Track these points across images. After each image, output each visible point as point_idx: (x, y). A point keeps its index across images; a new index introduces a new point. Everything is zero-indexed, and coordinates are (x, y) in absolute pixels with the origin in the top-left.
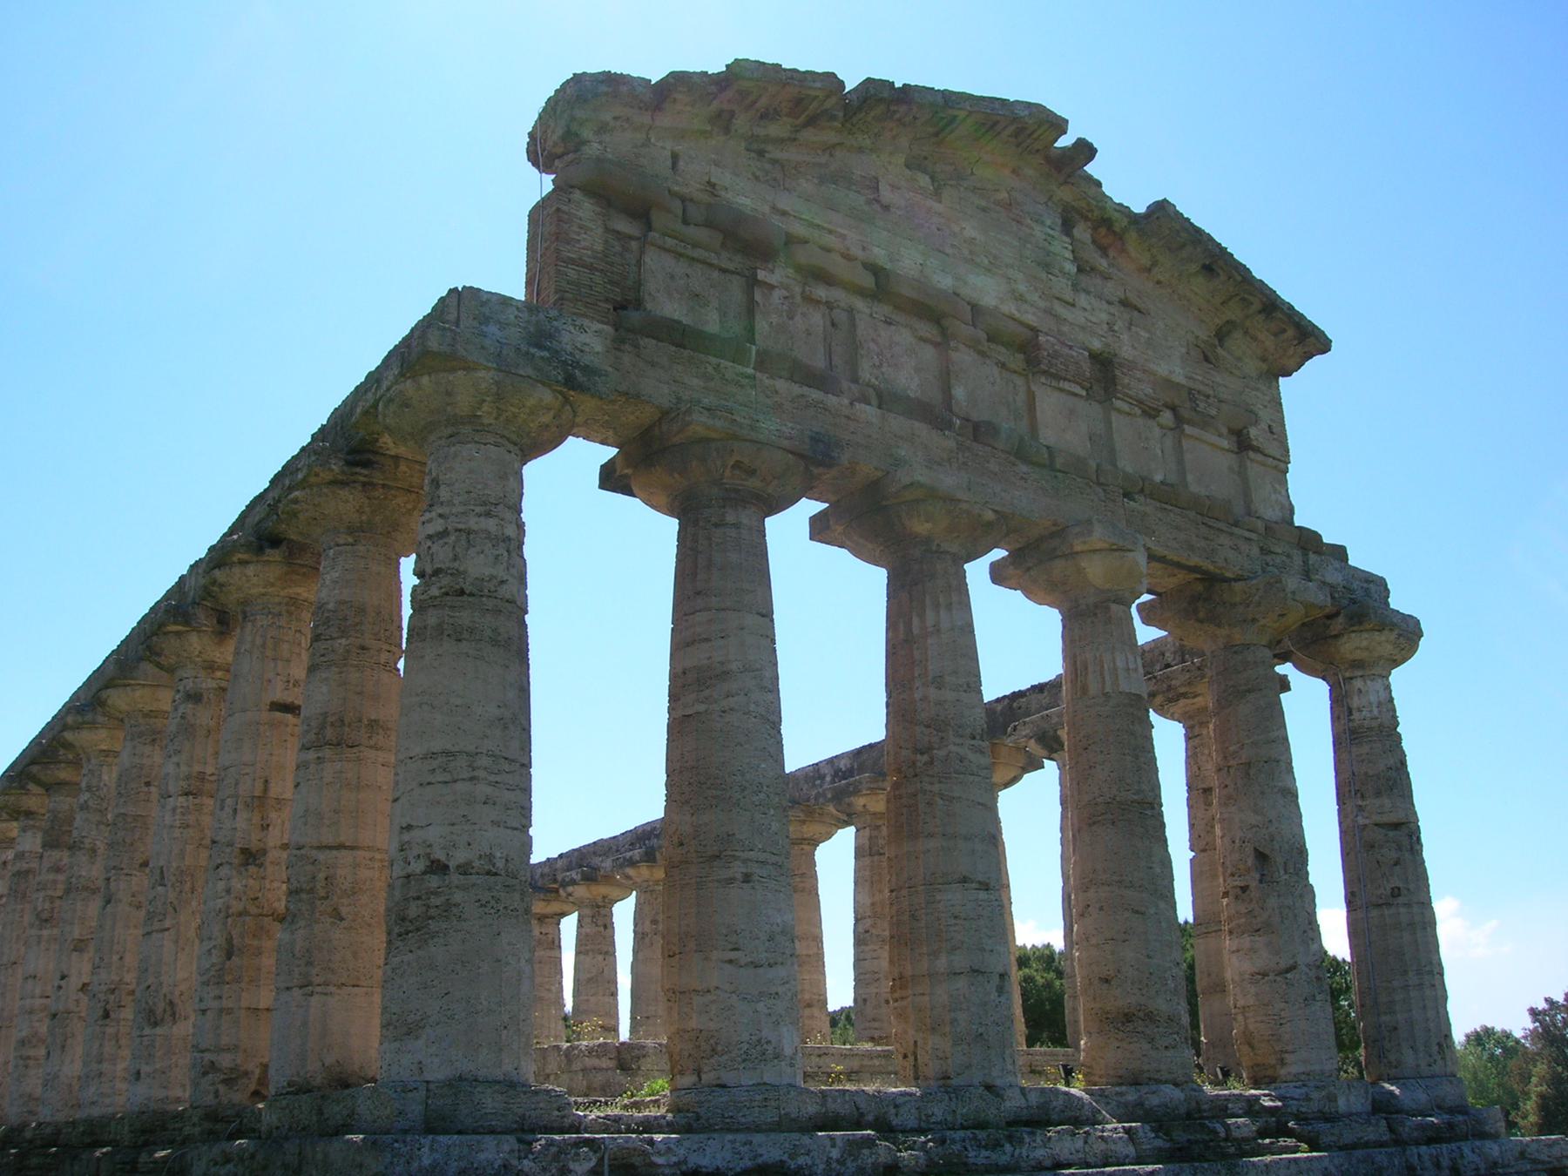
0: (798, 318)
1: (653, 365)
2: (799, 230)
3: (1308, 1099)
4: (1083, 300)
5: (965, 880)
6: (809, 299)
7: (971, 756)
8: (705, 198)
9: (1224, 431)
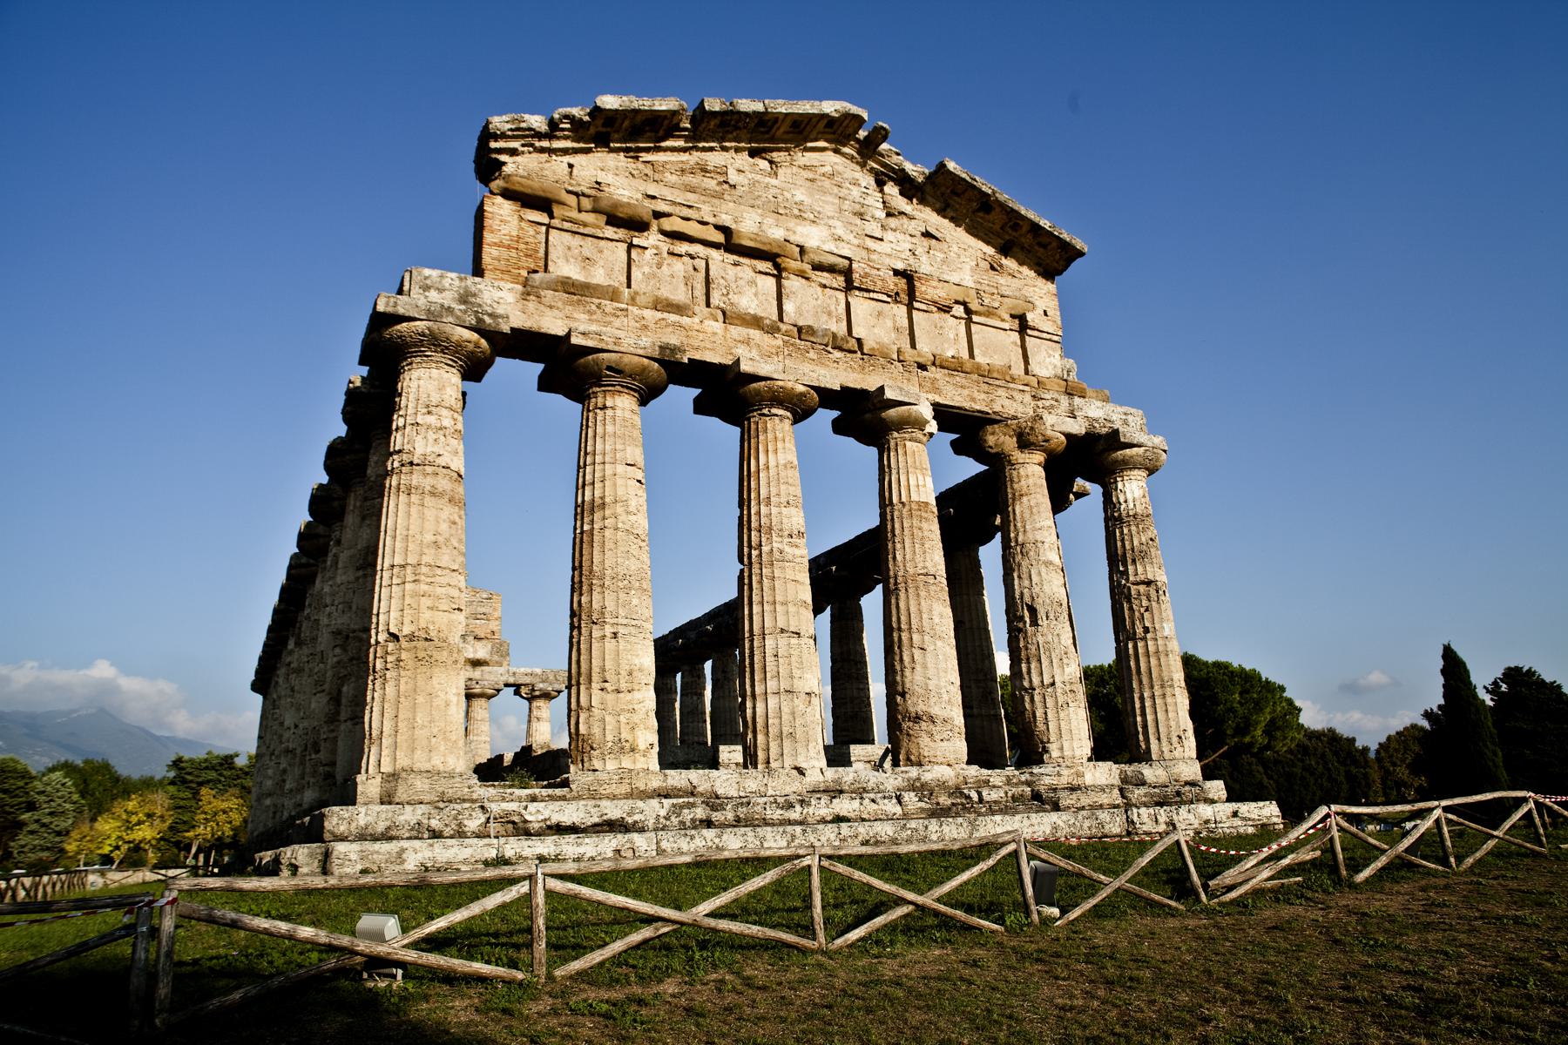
0: (664, 268)
1: (551, 307)
2: (662, 207)
3: (1059, 775)
4: (889, 236)
5: (782, 631)
6: (671, 254)
7: (787, 549)
8: (593, 192)
9: (1007, 317)
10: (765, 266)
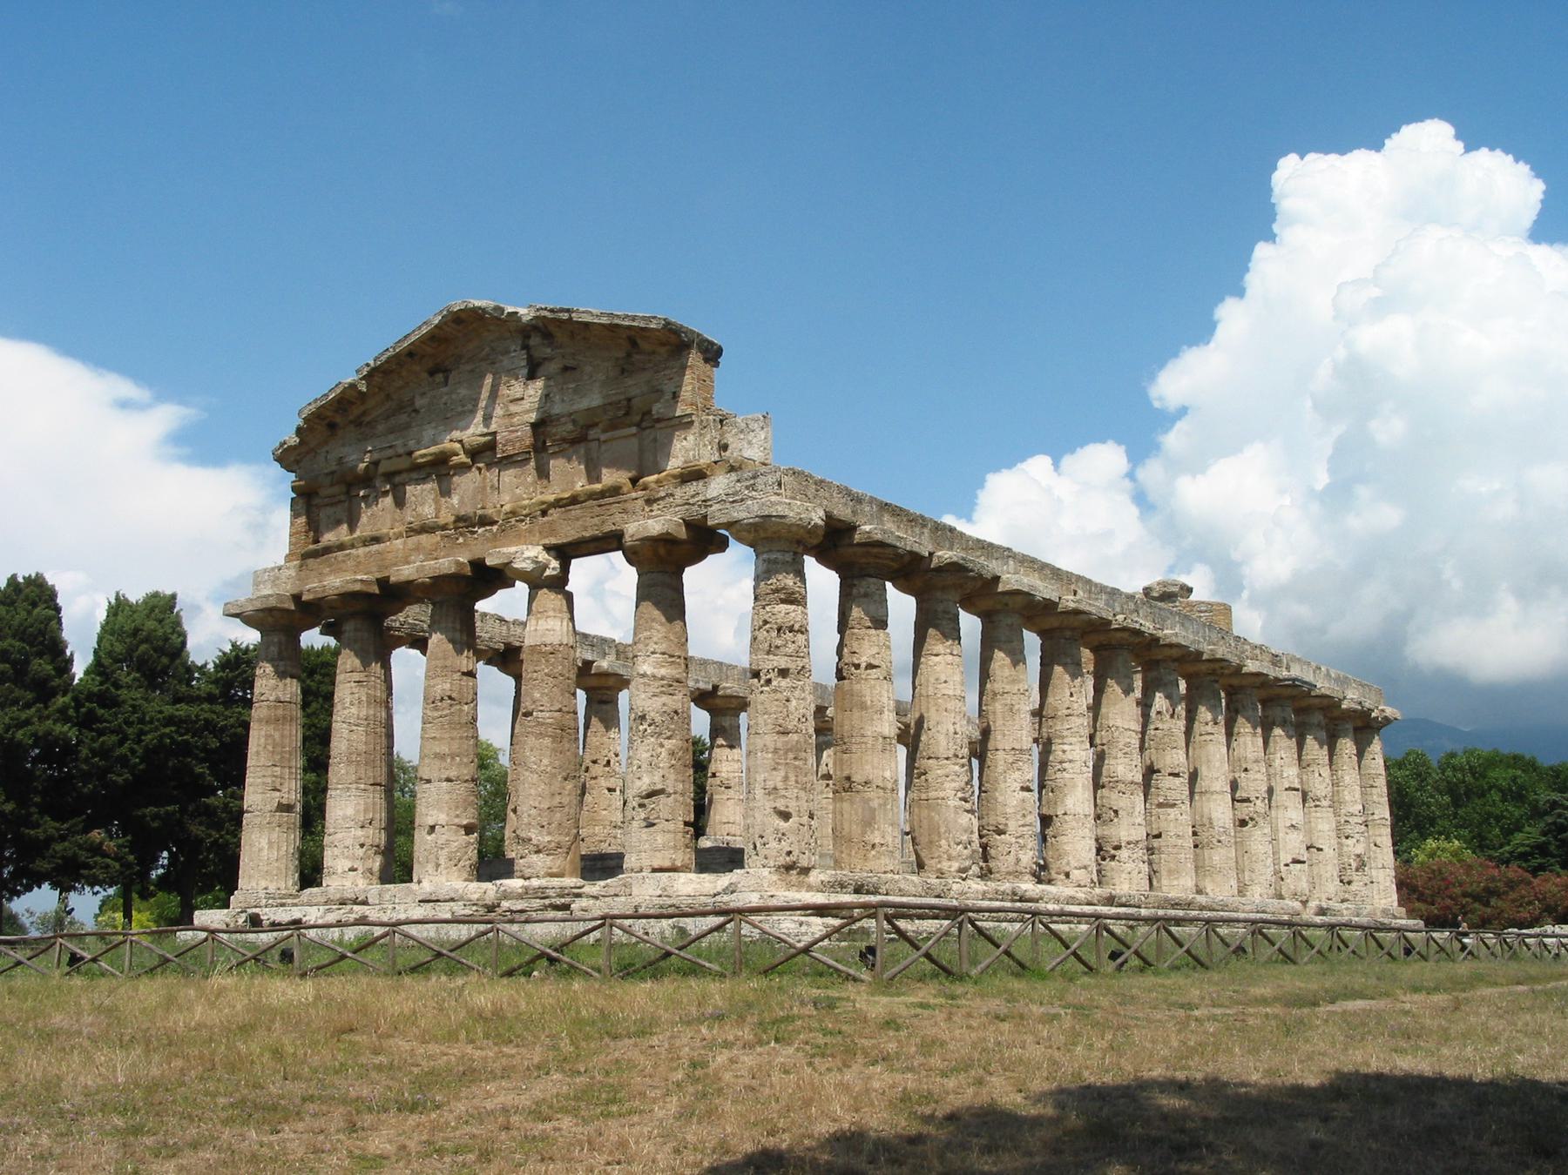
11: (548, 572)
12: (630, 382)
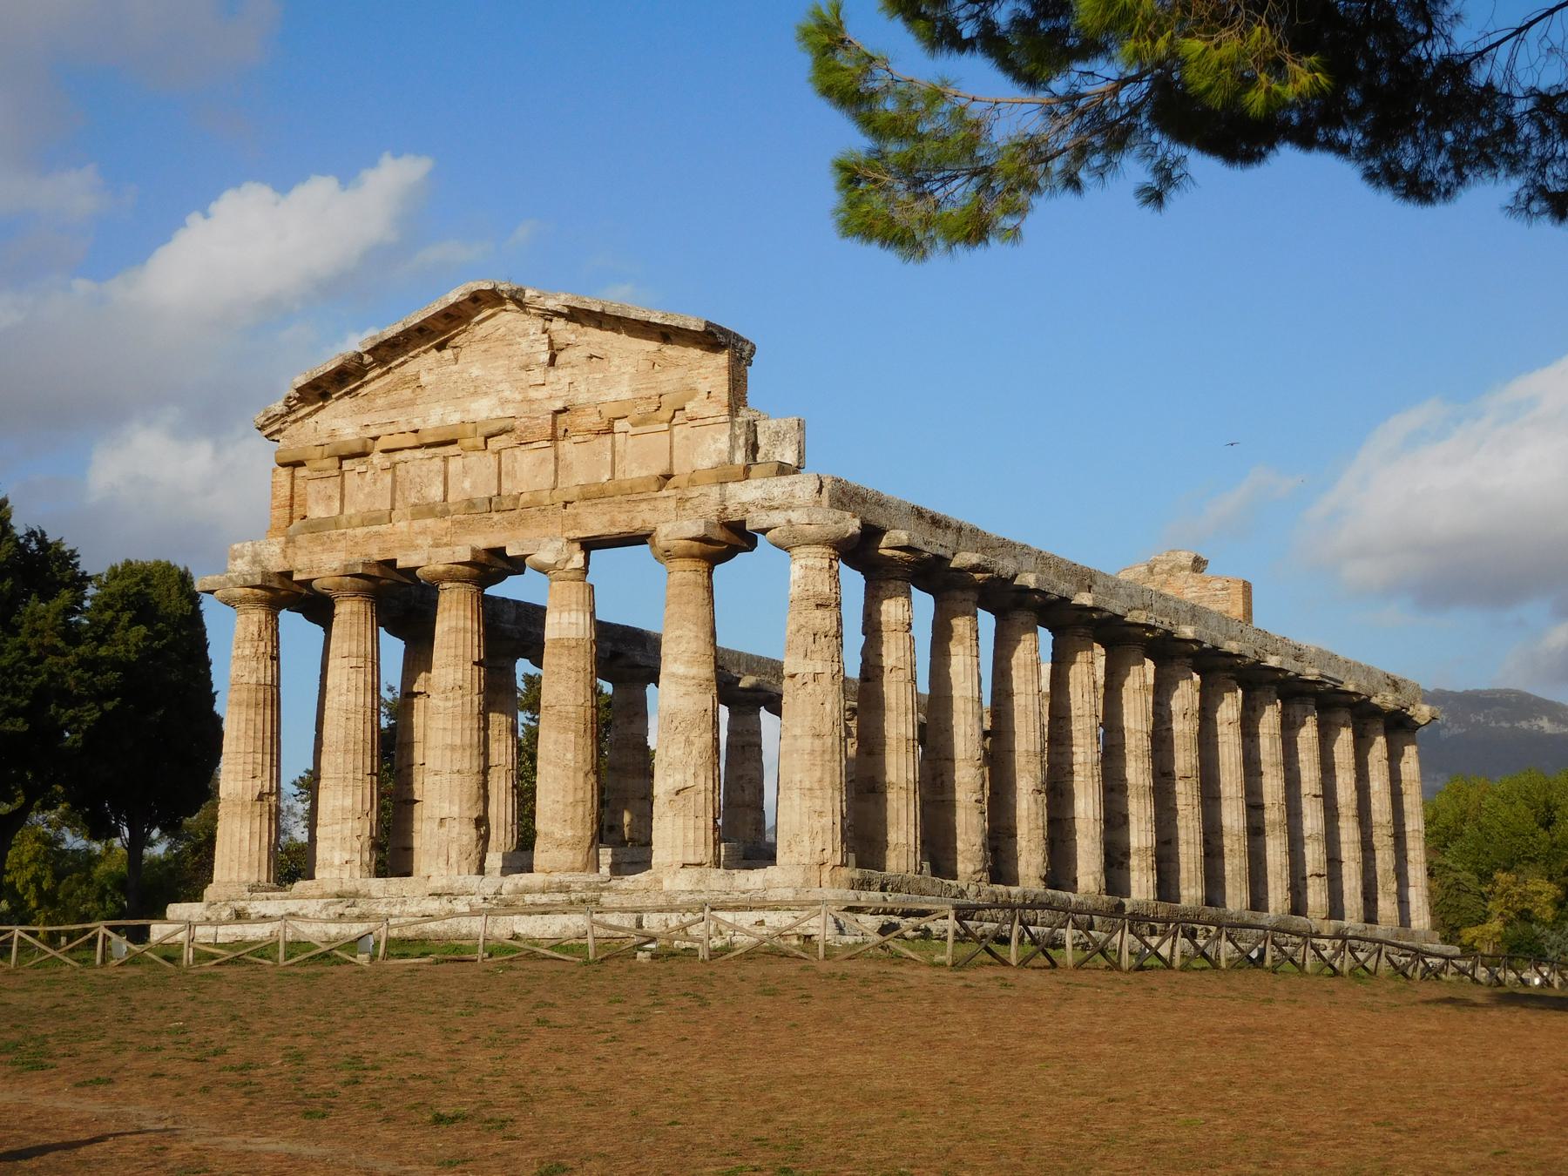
2: (373, 432)
4: (553, 374)
10: (451, 450)
11: (570, 566)
12: (662, 377)
